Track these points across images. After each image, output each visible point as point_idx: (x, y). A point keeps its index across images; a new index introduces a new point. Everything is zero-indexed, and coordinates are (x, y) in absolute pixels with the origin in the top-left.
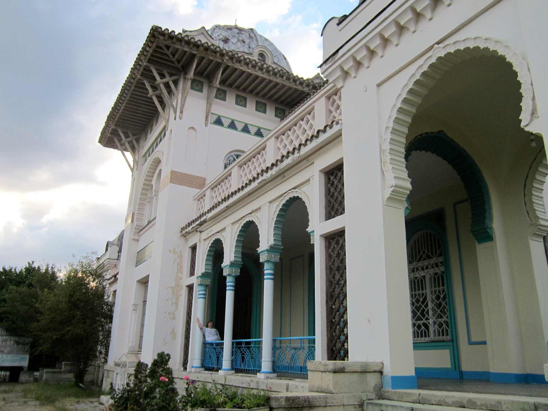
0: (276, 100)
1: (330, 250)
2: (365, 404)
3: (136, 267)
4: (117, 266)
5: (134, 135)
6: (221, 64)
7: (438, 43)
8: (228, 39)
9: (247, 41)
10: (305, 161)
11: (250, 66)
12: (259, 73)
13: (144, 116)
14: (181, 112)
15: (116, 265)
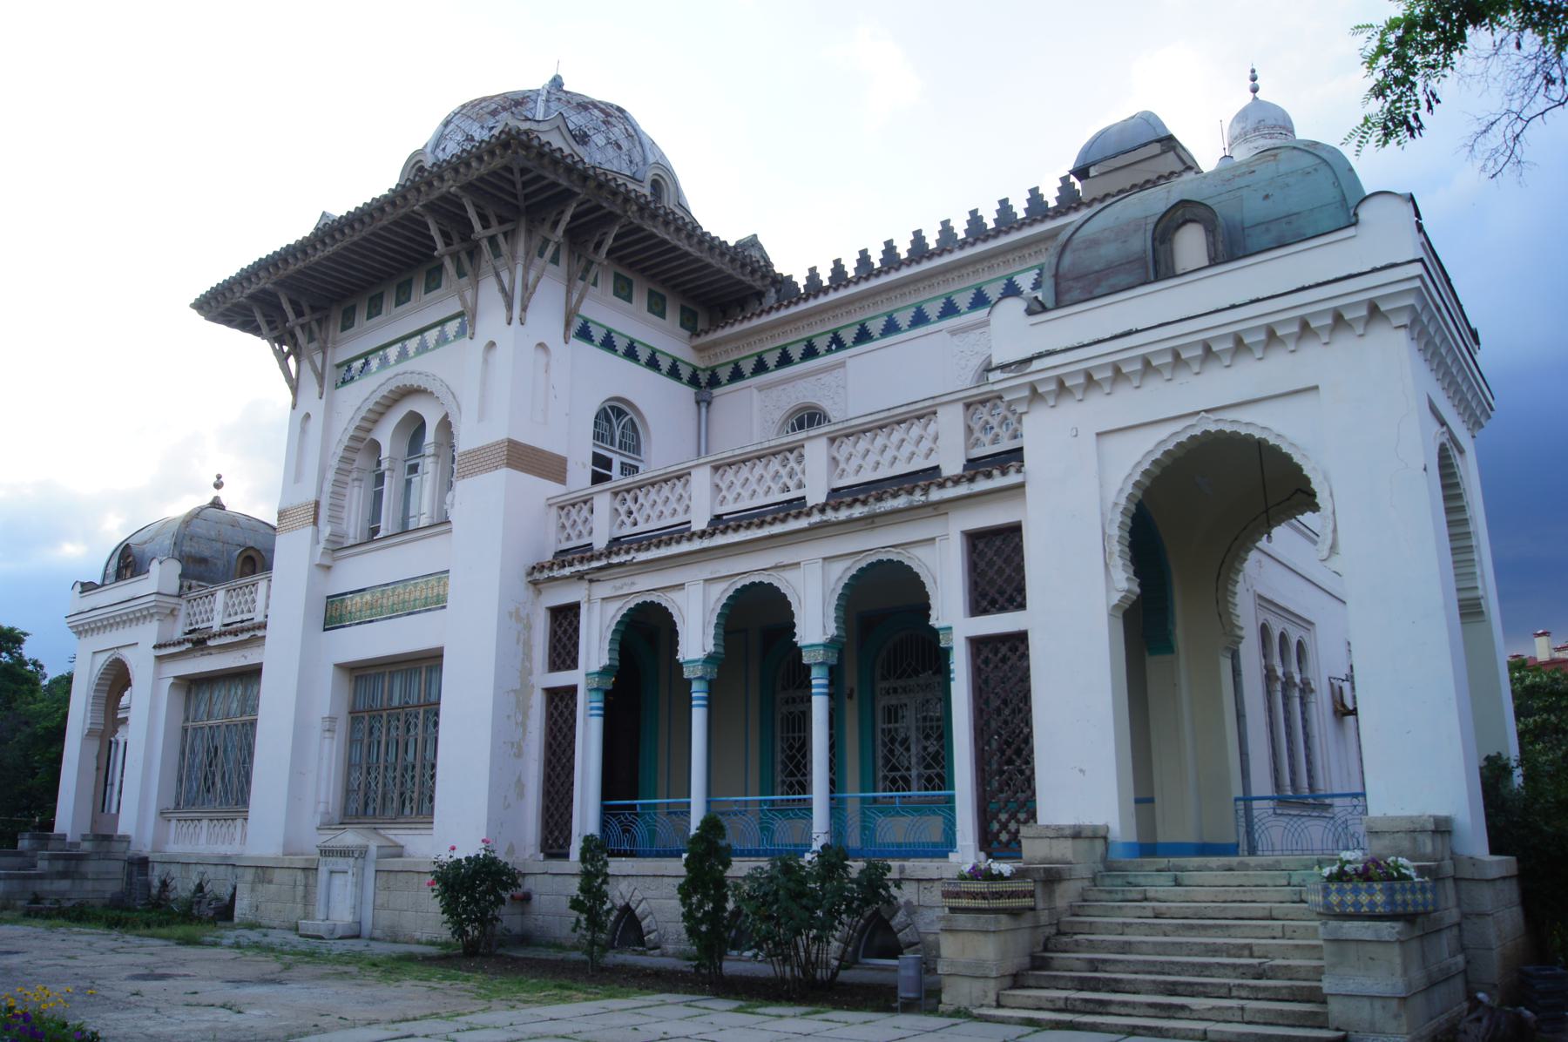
1: (979, 661)
2: (1099, 878)
3: (325, 630)
4: (176, 613)
5: (313, 309)
6: (618, 217)
7: (1206, 411)
8: (586, 135)
9: (625, 144)
10: (930, 509)
11: (672, 229)
13: (358, 274)
14: (524, 309)
15: (173, 611)
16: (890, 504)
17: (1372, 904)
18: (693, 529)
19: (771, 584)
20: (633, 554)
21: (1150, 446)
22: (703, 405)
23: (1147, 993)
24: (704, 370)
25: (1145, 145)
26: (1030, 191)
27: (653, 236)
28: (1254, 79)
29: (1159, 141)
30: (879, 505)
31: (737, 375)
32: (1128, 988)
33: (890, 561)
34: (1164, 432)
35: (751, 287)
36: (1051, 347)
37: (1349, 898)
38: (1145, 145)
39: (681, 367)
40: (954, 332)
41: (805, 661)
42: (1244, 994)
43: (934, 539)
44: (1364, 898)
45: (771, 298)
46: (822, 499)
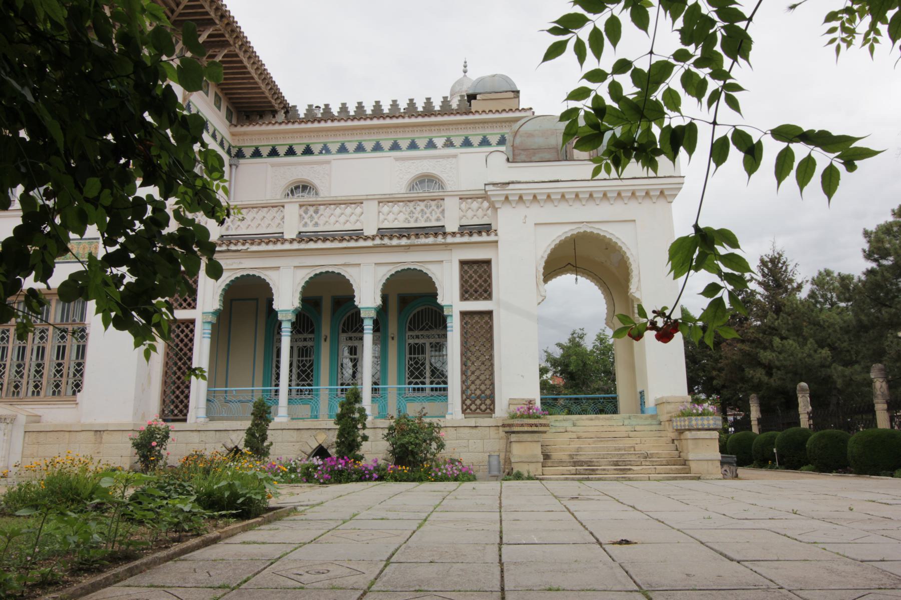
0: (230, 99)
6: (230, 45)
12: (253, 72)
16: (423, 240)
17: (709, 424)
18: (285, 237)
19: (339, 274)
20: (247, 246)
21: (560, 233)
22: (234, 167)
23: (605, 465)
24: (233, 147)
25: (506, 92)
26: (444, 98)
27: (241, 62)
28: (465, 67)
29: (513, 92)
30: (417, 240)
31: (257, 154)
32: (596, 464)
33: (415, 269)
34: (567, 228)
35: (273, 106)
36: (519, 180)
37: (700, 422)
38: (506, 92)
39: (225, 142)
40: (397, 159)
41: (362, 315)
42: (647, 464)
43: (442, 261)
44: (706, 422)
45: (281, 116)
46: (374, 232)
